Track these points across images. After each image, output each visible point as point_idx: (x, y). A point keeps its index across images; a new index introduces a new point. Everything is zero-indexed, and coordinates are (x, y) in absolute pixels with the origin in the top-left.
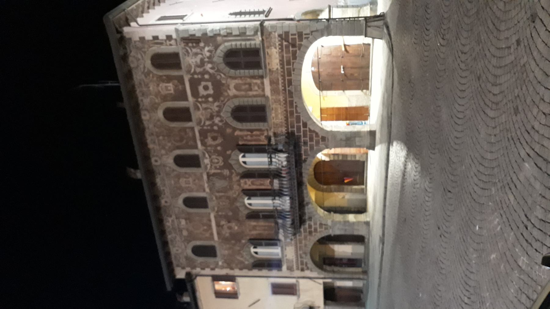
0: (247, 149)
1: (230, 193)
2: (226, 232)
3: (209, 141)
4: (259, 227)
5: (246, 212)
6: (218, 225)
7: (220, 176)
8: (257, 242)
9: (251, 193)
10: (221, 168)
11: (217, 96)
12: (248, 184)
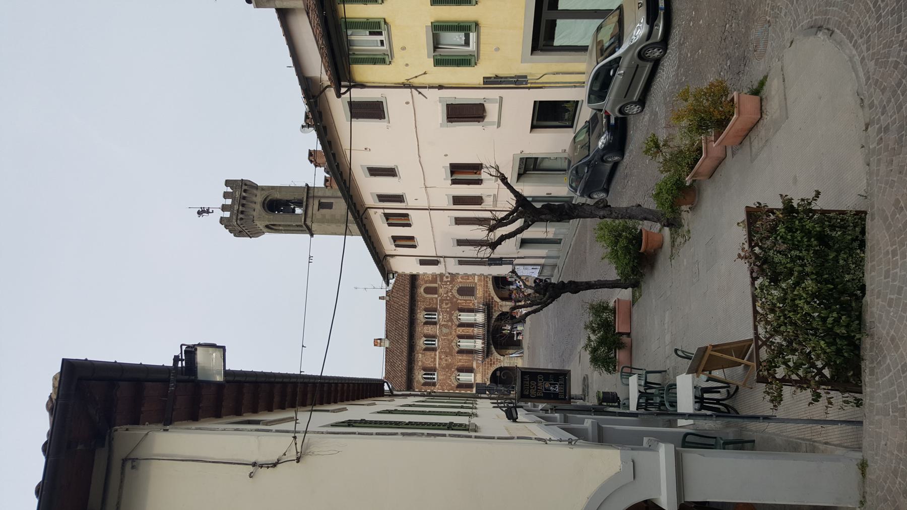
0: (462, 310)
1: (450, 337)
2: (444, 363)
3: (444, 306)
4: (462, 360)
5: (457, 349)
6: (440, 359)
7: (446, 326)
8: (461, 370)
9: (461, 337)
10: (448, 321)
11: (451, 282)
12: (461, 331)
